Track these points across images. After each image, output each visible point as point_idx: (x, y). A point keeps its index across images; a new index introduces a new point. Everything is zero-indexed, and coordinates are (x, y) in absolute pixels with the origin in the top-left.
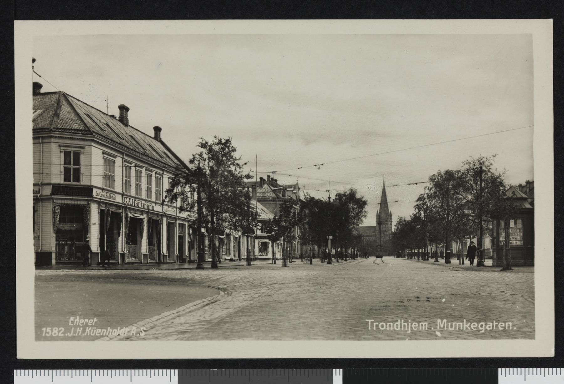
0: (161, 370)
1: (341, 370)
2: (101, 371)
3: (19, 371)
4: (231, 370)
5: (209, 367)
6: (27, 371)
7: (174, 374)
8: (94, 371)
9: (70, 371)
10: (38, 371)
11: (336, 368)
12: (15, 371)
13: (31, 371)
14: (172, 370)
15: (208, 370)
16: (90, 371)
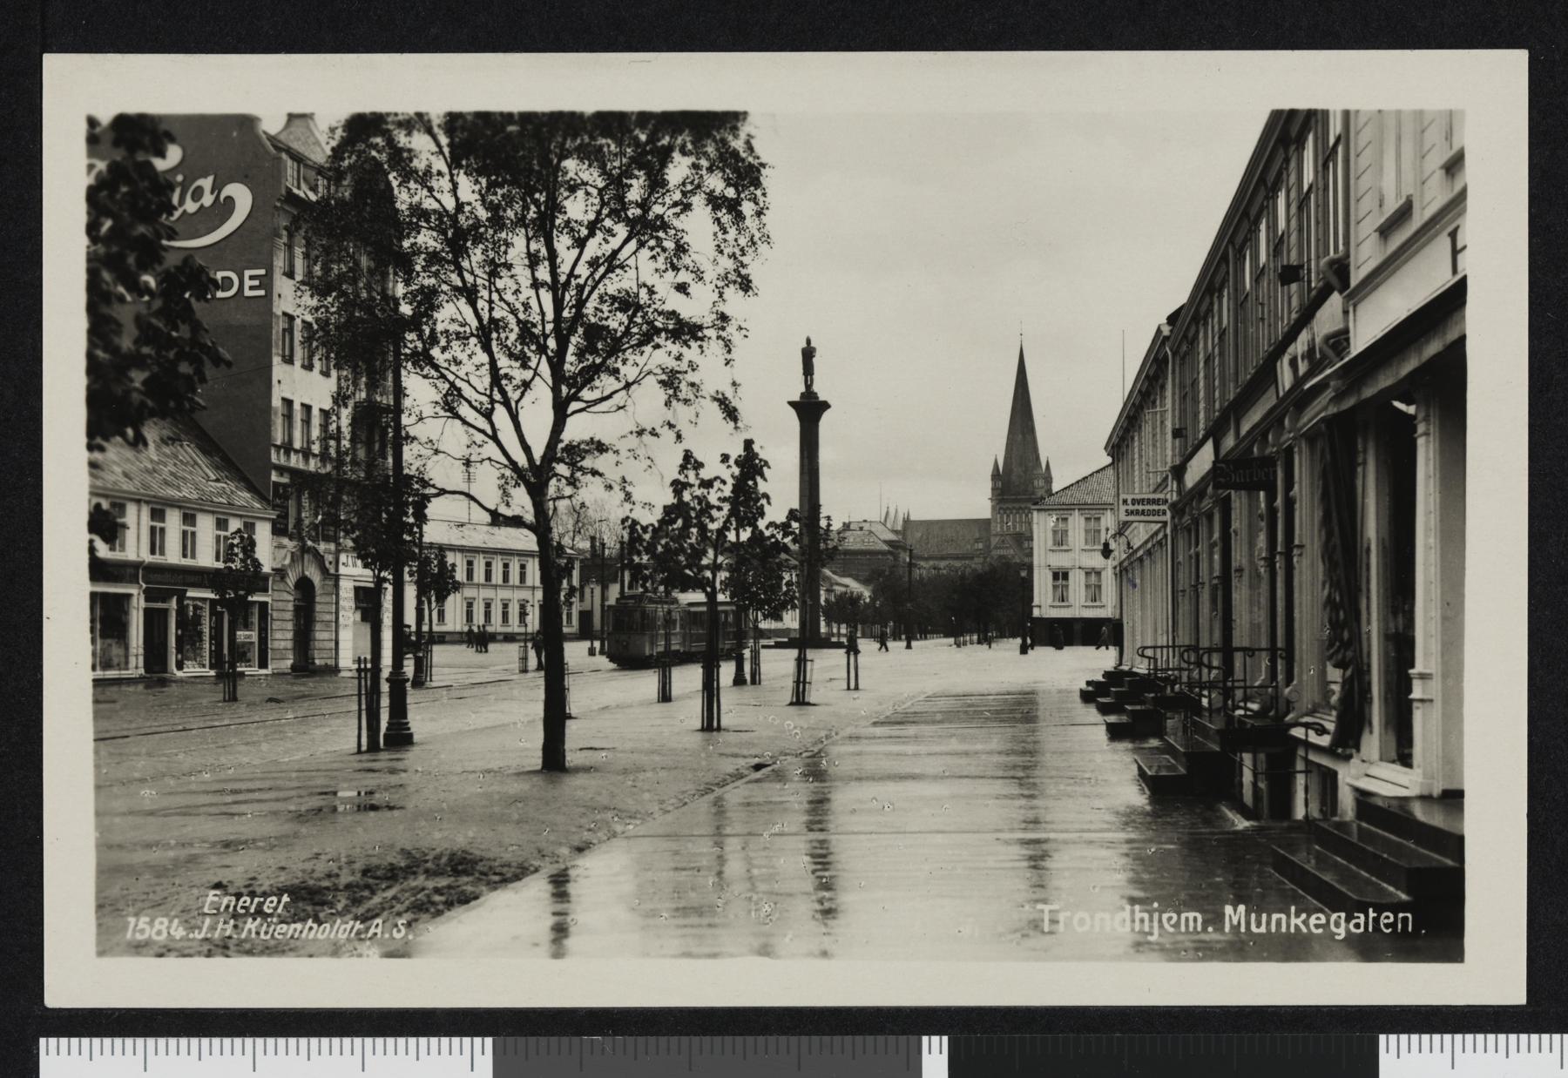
0: (445, 1040)
1: (945, 1039)
2: (281, 1041)
3: (53, 1041)
4: (641, 1039)
5: (579, 1033)
6: (75, 1041)
7: (483, 1048)
8: (260, 1041)
9: (194, 1041)
10: (107, 1041)
11: (930, 1033)
12: (42, 1041)
13: (85, 1041)
14: (478, 1040)
15: (576, 1040)
16: (249, 1041)
